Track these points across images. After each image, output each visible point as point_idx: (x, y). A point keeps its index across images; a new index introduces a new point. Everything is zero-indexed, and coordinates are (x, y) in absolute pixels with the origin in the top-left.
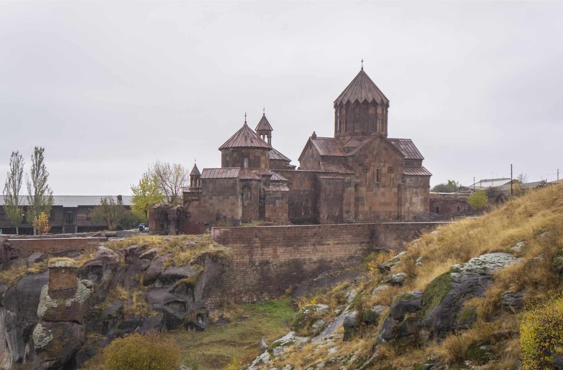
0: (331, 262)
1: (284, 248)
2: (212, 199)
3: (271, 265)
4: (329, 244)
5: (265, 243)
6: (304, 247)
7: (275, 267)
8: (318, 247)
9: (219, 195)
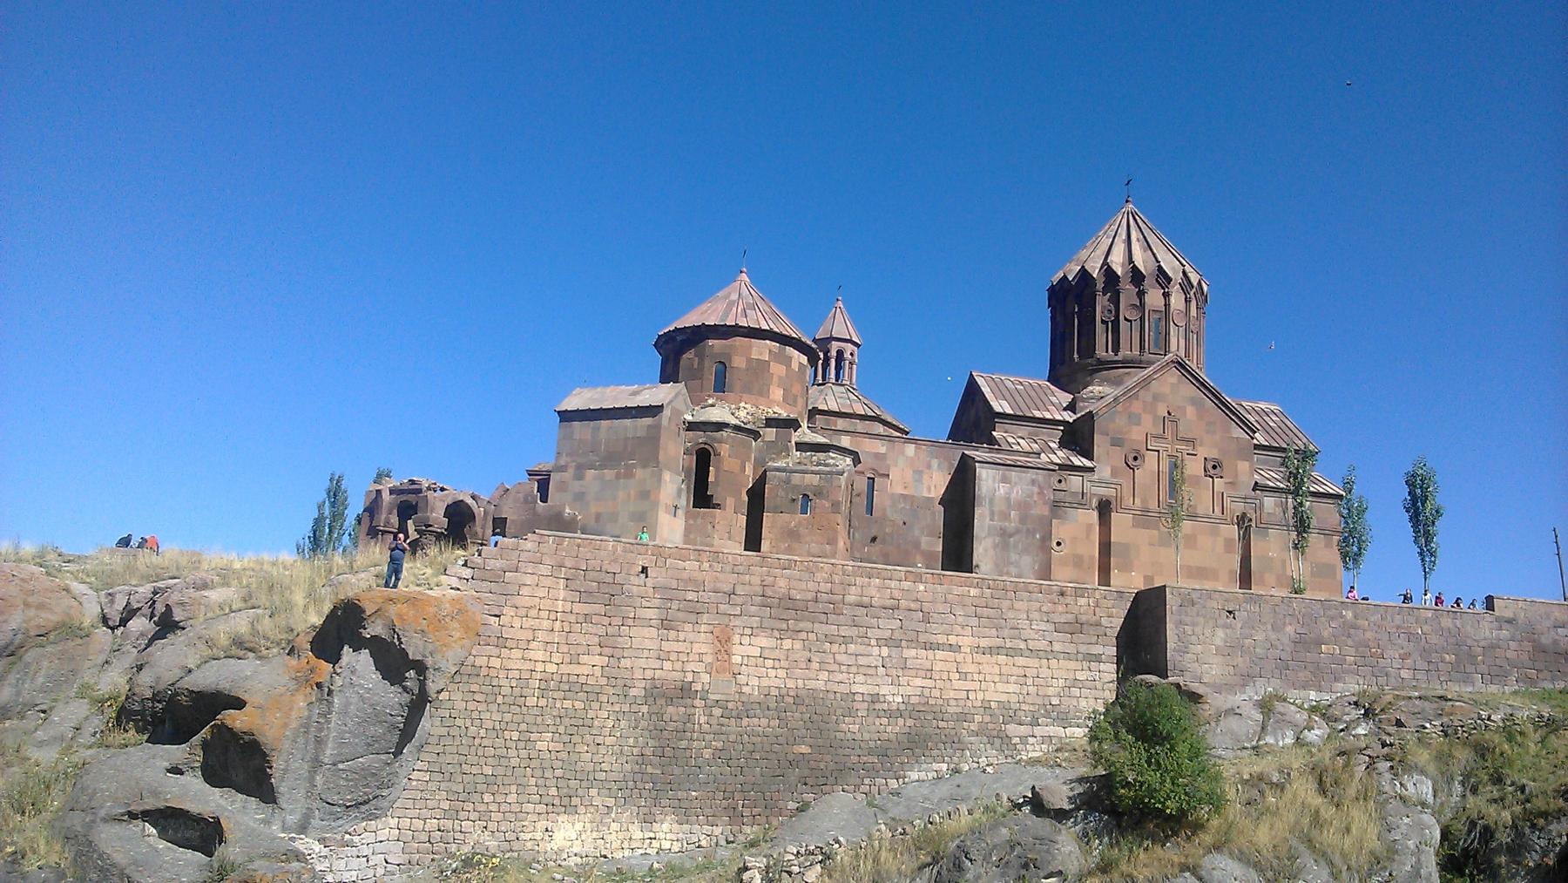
0: (963, 717)
1: (763, 641)
2: (579, 476)
3: (697, 702)
4: (956, 648)
7: (717, 712)
9: (603, 467)
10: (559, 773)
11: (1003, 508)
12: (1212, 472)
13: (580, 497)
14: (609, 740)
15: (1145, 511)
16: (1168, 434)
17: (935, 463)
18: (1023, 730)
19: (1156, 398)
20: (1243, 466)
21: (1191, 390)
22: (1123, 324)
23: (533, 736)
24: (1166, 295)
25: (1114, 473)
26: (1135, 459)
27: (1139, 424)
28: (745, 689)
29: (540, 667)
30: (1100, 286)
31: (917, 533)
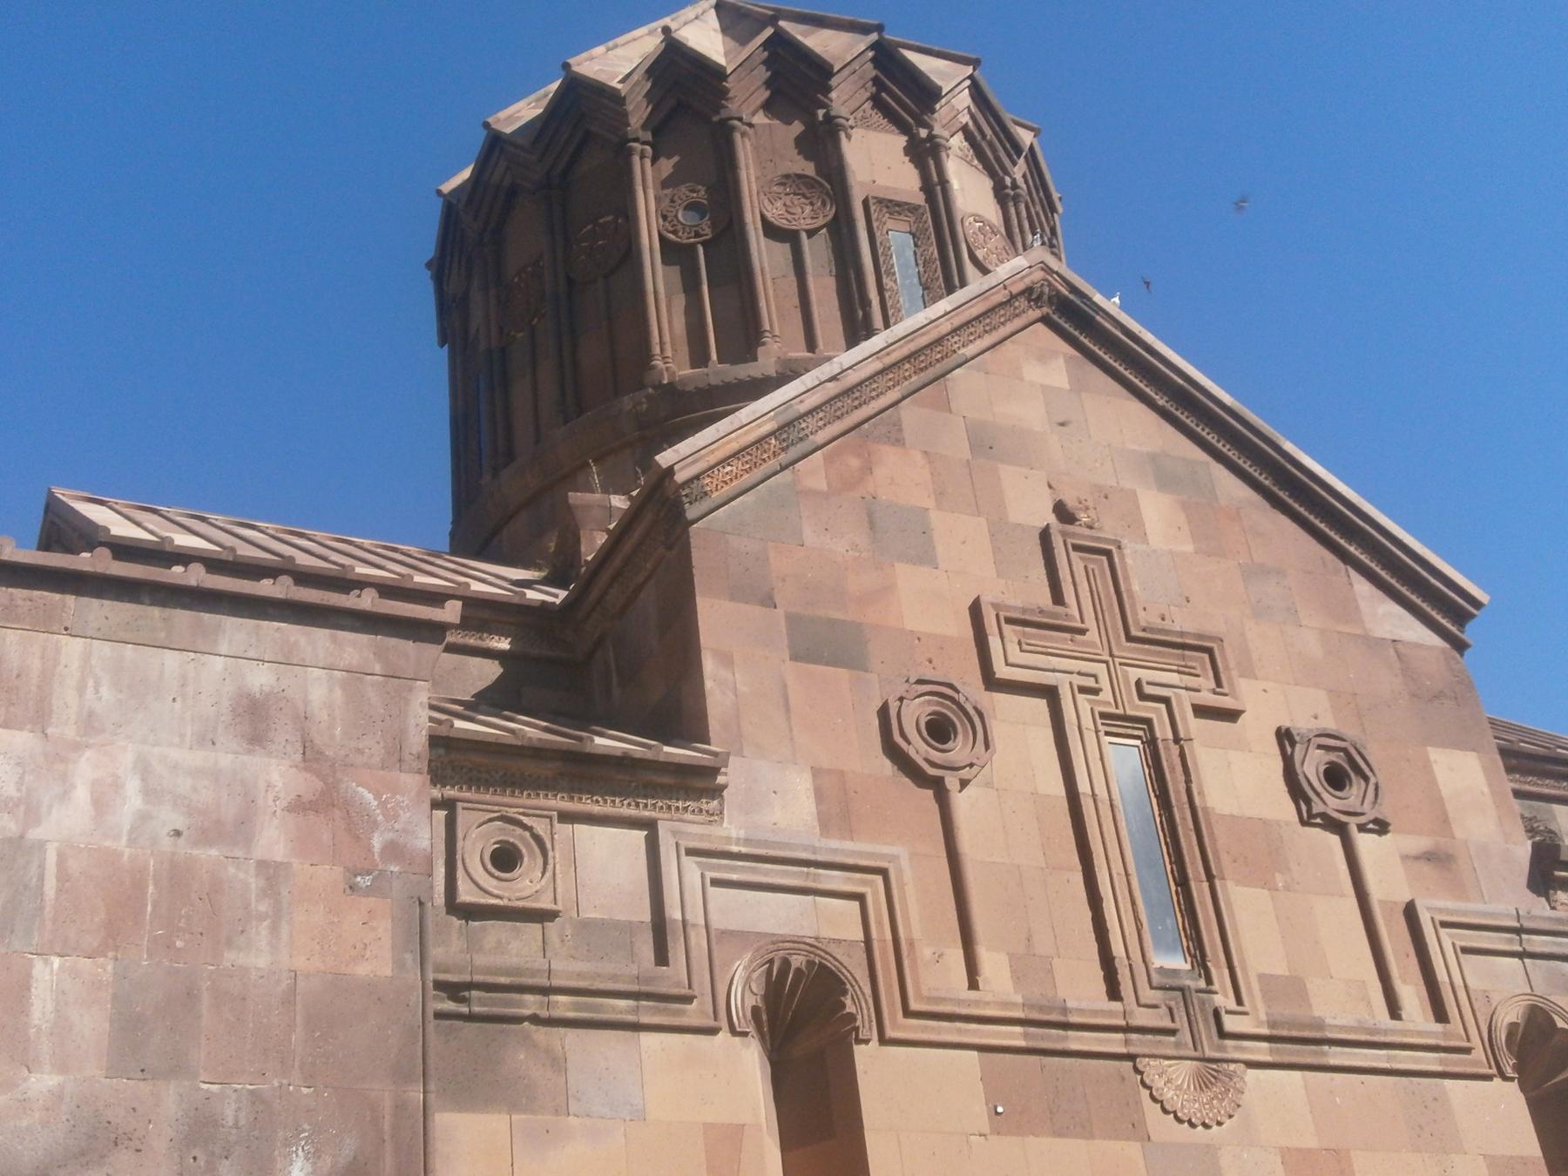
12: (1331, 802)
16: (1079, 605)
19: (986, 444)
21: (1132, 426)
22: (767, 257)
24: (925, 154)
26: (939, 730)
27: (926, 557)
30: (638, 113)
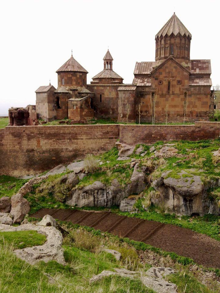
0: (84, 151)
1: (46, 141)
4: (82, 139)
5: (29, 138)
6: (62, 141)
7: (39, 153)
8: (73, 141)
10: (14, 164)
11: (124, 99)
12: (178, 83)
13: (39, 108)
14: (21, 159)
15: (162, 94)
17: (113, 90)
18: (96, 152)
20: (186, 81)
23: (9, 159)
25: (156, 86)
28: (43, 149)
29: (9, 148)
31: (110, 105)
